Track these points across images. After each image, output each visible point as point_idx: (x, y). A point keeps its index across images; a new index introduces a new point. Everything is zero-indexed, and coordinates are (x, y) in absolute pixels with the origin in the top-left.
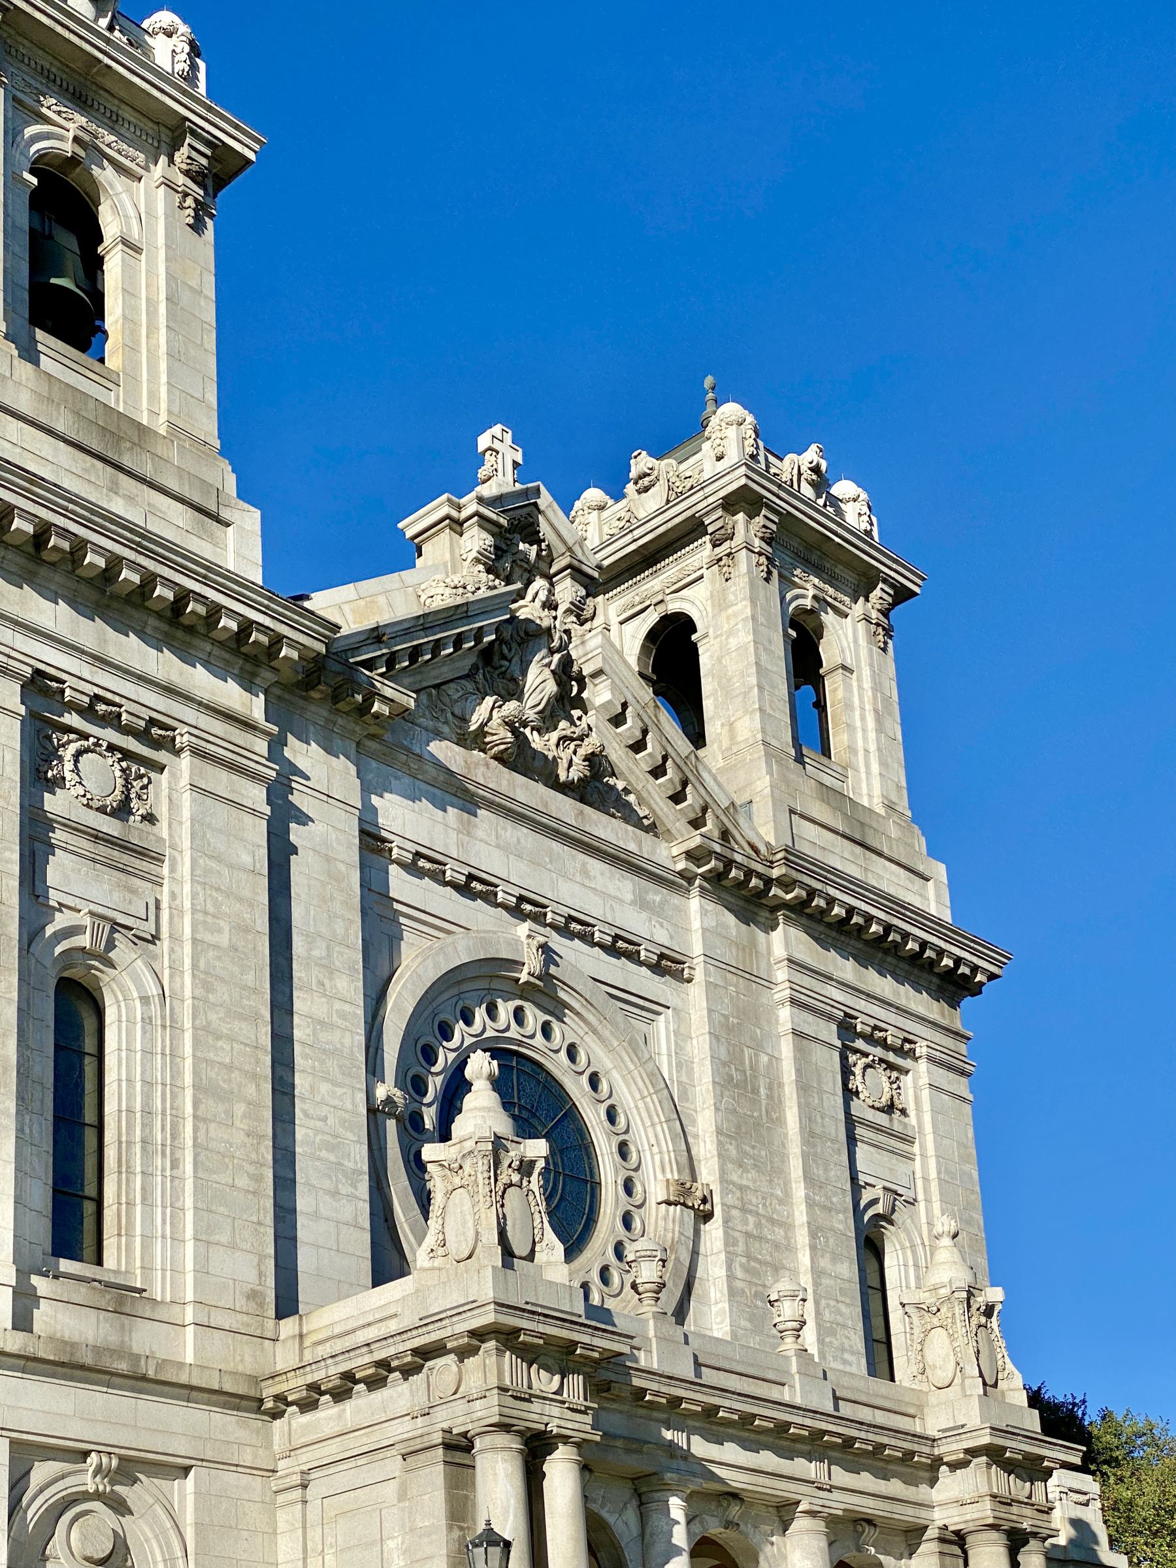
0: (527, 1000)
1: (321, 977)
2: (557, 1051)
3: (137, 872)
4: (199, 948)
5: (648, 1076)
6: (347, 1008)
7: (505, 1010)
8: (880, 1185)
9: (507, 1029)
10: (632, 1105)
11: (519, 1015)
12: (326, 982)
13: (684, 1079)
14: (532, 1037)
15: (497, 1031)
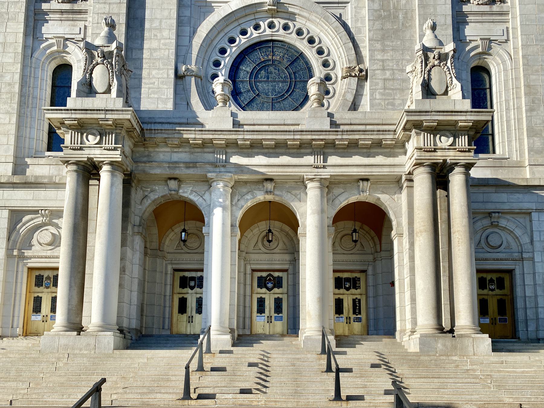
0: (275, 18)
1: (155, 33)
2: (291, 33)
3: (78, 19)
4: (94, 36)
5: (334, 29)
6: (167, 41)
7: (263, 25)
8: (478, 38)
9: (265, 31)
10: (330, 44)
11: (271, 26)
12: (159, 35)
13: (359, 25)
14: (278, 31)
15: (259, 33)
